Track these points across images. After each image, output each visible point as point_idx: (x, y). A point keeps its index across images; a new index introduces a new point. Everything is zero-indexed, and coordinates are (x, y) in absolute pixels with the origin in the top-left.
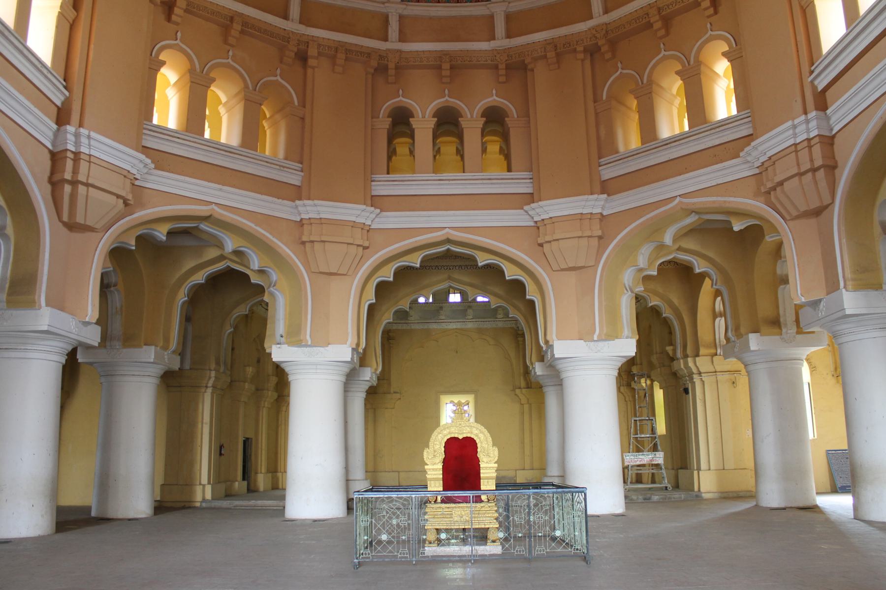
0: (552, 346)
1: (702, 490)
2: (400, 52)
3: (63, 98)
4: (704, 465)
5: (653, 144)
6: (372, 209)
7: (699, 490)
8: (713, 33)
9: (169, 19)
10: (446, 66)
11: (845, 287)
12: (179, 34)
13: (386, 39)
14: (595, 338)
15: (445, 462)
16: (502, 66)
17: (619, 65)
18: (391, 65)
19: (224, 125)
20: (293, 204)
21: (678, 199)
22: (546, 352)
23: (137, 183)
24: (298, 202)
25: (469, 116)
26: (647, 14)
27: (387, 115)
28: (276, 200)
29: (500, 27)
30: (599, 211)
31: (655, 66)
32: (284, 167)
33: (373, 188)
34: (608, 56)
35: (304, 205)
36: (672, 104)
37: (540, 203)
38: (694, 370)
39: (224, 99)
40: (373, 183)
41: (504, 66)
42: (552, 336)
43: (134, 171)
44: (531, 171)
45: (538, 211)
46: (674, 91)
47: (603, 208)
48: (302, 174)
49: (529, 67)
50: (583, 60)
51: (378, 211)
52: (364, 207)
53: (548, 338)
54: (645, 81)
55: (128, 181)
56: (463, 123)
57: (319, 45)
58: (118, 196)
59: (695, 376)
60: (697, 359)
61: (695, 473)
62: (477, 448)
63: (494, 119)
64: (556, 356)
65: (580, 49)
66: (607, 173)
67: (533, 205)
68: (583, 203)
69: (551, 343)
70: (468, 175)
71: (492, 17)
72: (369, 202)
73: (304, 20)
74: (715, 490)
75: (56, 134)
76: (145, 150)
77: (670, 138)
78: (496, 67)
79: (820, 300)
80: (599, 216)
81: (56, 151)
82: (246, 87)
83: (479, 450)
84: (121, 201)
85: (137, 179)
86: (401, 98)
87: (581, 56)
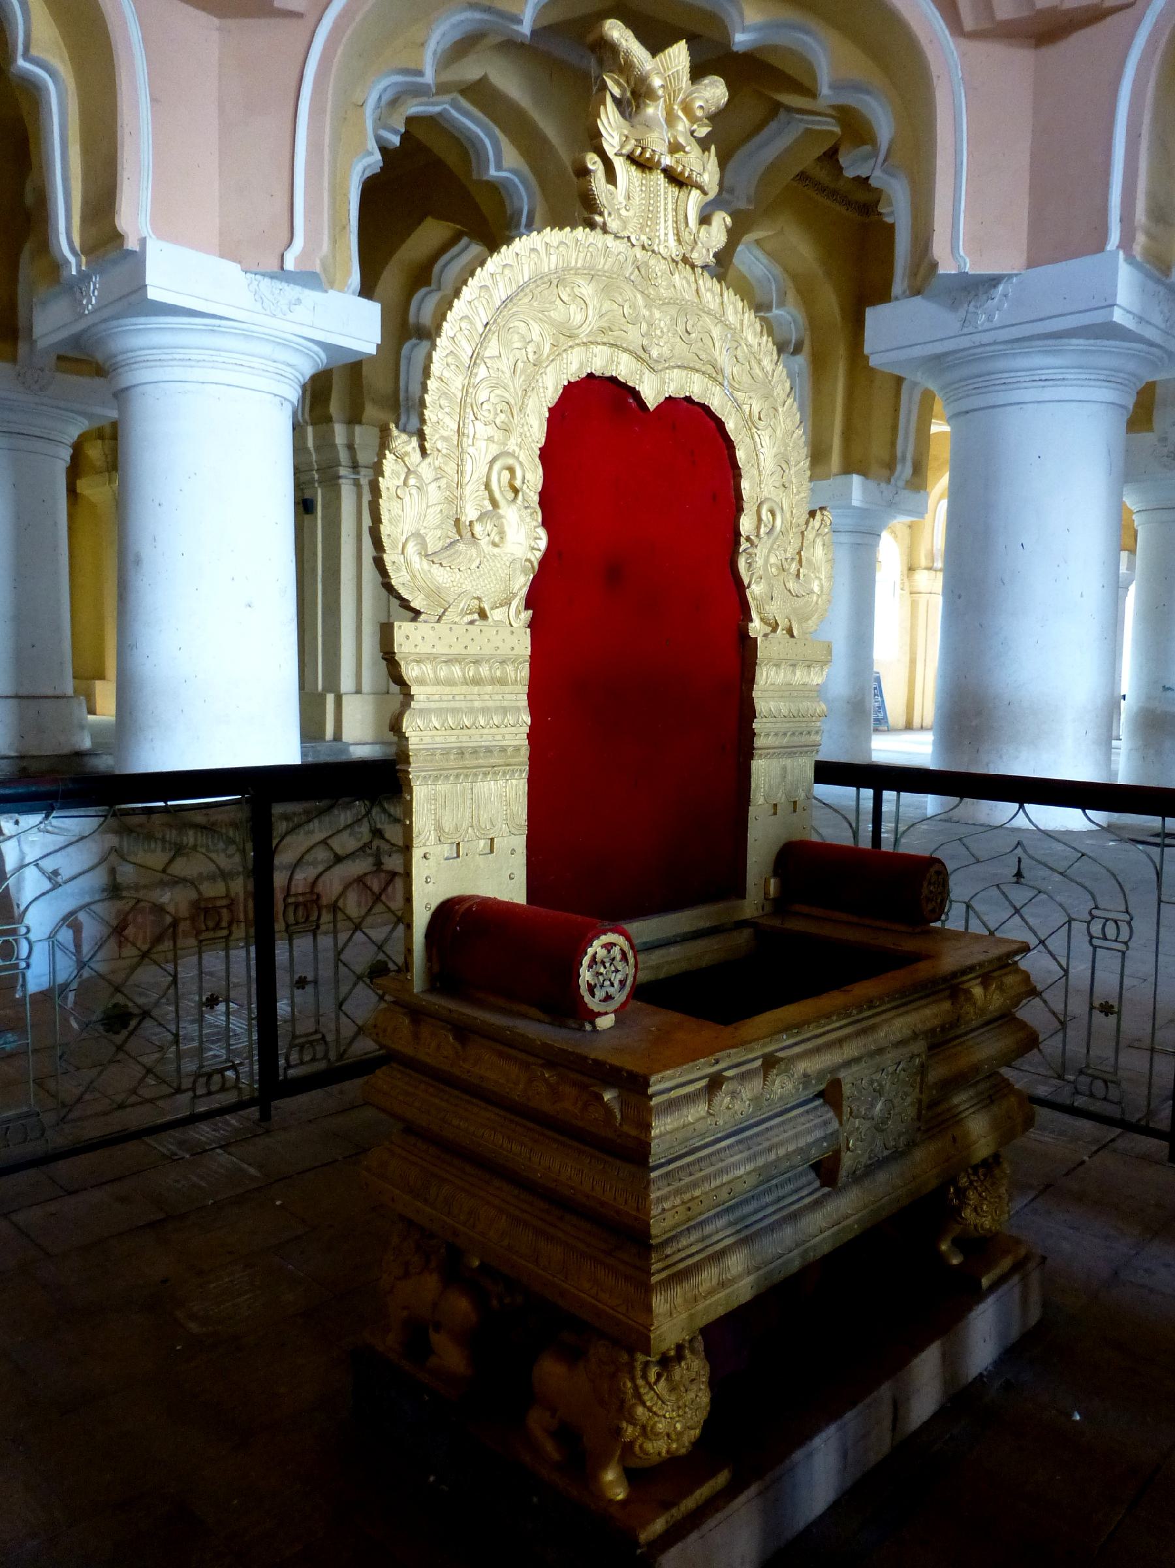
0: (137, 260)
1: (347, 737)
4: (347, 682)
7: (338, 737)
11: (1126, 243)
14: (289, 265)
15: (545, 595)
22: (75, 288)
38: (343, 455)
42: (135, 217)
53: (124, 222)
59: (343, 472)
60: (358, 429)
61: (330, 698)
62: (737, 506)
64: (152, 294)
69: (131, 244)
74: (369, 739)
79: (994, 281)
83: (746, 524)
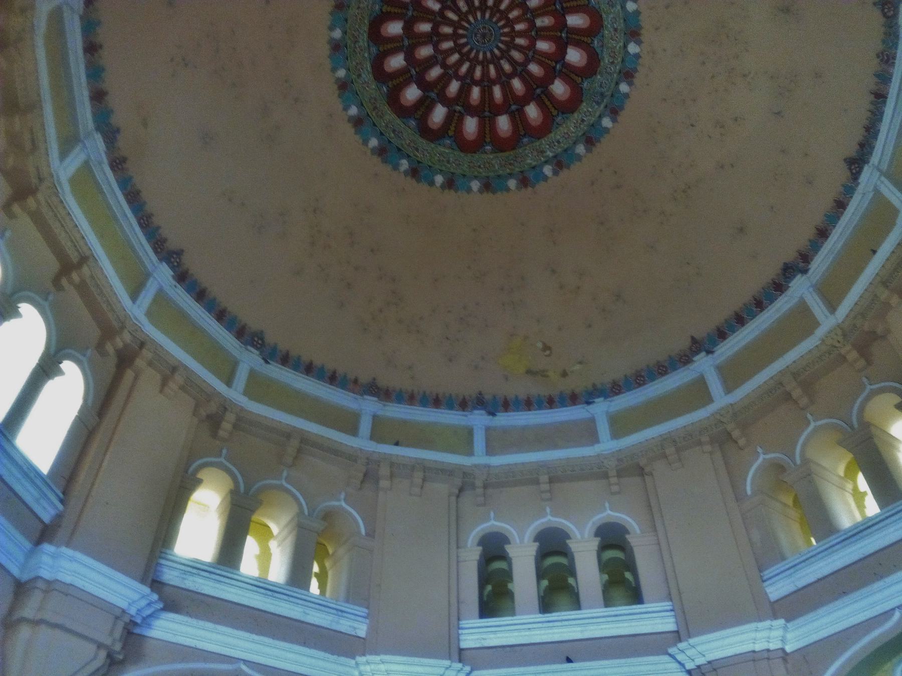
2: (488, 466)
3: (53, 512)
5: (833, 539)
6: (460, 665)
8: (872, 387)
9: (214, 435)
10: (544, 478)
12: (224, 451)
13: (470, 453)
16: (613, 473)
17: (759, 450)
18: (479, 483)
19: (267, 557)
20: (353, 662)
21: (897, 615)
23: (137, 631)
24: (361, 659)
25: (579, 536)
26: (781, 384)
27: (476, 541)
28: (329, 656)
29: (603, 429)
30: (779, 645)
31: (804, 445)
32: (342, 611)
33: (462, 637)
34: (742, 442)
35: (368, 663)
36: (843, 489)
37: (692, 641)
39: (275, 528)
40: (460, 631)
41: (614, 473)
43: (133, 611)
44: (671, 600)
45: (689, 653)
46: (841, 471)
47: (784, 640)
48: (367, 621)
49: (647, 470)
50: (711, 453)
51: (467, 669)
52: (447, 663)
54: (798, 462)
55: (120, 625)
56: (573, 545)
57: (392, 465)
58: (100, 646)
63: (612, 539)
65: (705, 439)
66: (777, 590)
67: (682, 645)
68: (753, 635)
70: (584, 613)
71: (592, 420)
72: (456, 657)
73: (375, 436)
75: (30, 555)
76: (156, 585)
77: (856, 526)
78: (606, 476)
80: (781, 654)
81: (25, 577)
82: (301, 513)
84: (103, 654)
85: (135, 624)
86: (493, 522)
87: (708, 448)
